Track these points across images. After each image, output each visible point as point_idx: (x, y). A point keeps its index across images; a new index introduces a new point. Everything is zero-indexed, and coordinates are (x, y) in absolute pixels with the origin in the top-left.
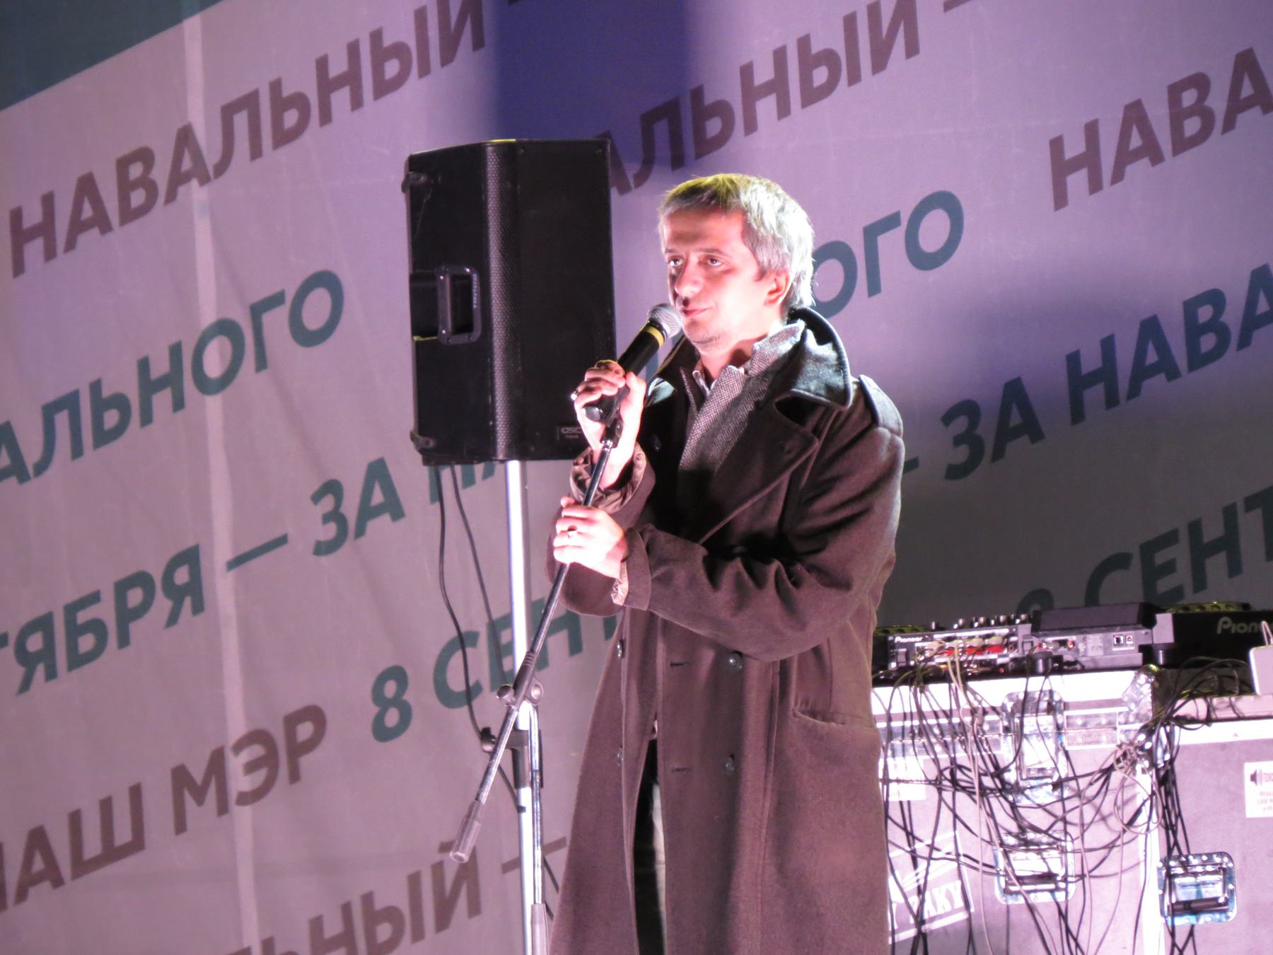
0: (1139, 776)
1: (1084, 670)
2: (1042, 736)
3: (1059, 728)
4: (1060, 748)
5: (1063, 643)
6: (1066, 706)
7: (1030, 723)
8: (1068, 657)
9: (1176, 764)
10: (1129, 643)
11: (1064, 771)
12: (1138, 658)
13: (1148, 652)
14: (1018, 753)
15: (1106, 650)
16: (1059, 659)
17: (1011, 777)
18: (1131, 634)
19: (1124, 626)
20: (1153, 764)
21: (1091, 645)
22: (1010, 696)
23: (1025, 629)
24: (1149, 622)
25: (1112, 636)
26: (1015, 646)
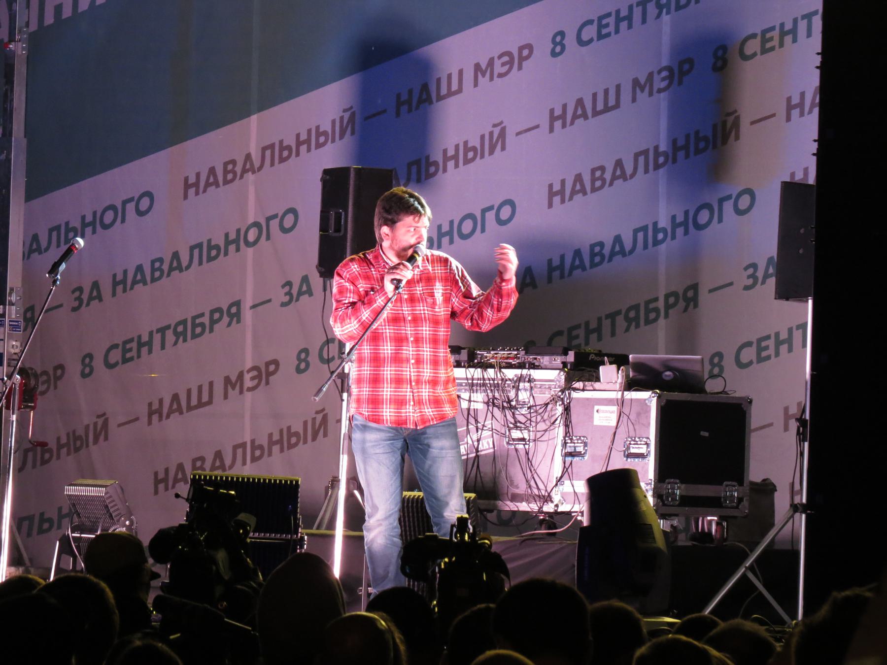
0: (558, 407)
1: (542, 369)
2: (526, 390)
3: (531, 388)
4: (531, 395)
5: (536, 359)
6: (535, 380)
7: (521, 385)
8: (537, 364)
9: (571, 404)
10: (558, 360)
11: (532, 403)
12: (561, 366)
13: (565, 364)
14: (517, 395)
15: (550, 363)
16: (533, 364)
17: (513, 403)
18: (559, 357)
19: (557, 354)
20: (563, 403)
21: (545, 360)
22: (516, 376)
23: (523, 353)
24: (566, 354)
25: (553, 358)
26: (519, 358)
